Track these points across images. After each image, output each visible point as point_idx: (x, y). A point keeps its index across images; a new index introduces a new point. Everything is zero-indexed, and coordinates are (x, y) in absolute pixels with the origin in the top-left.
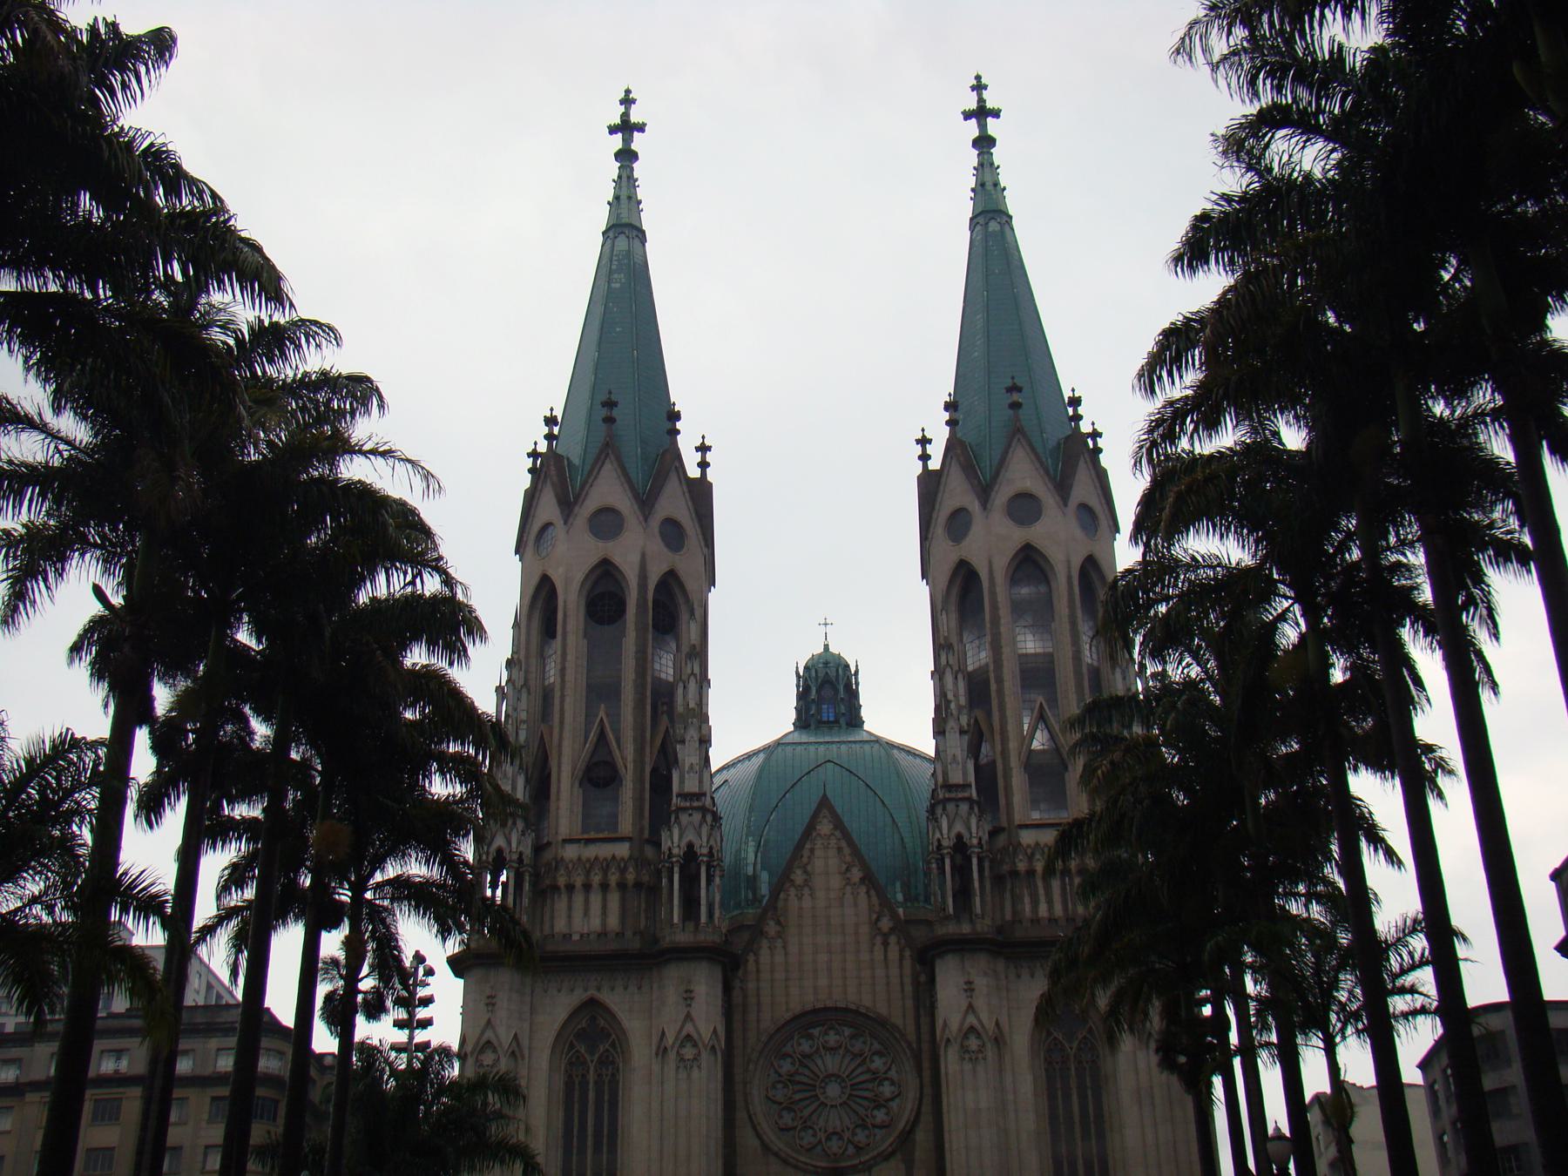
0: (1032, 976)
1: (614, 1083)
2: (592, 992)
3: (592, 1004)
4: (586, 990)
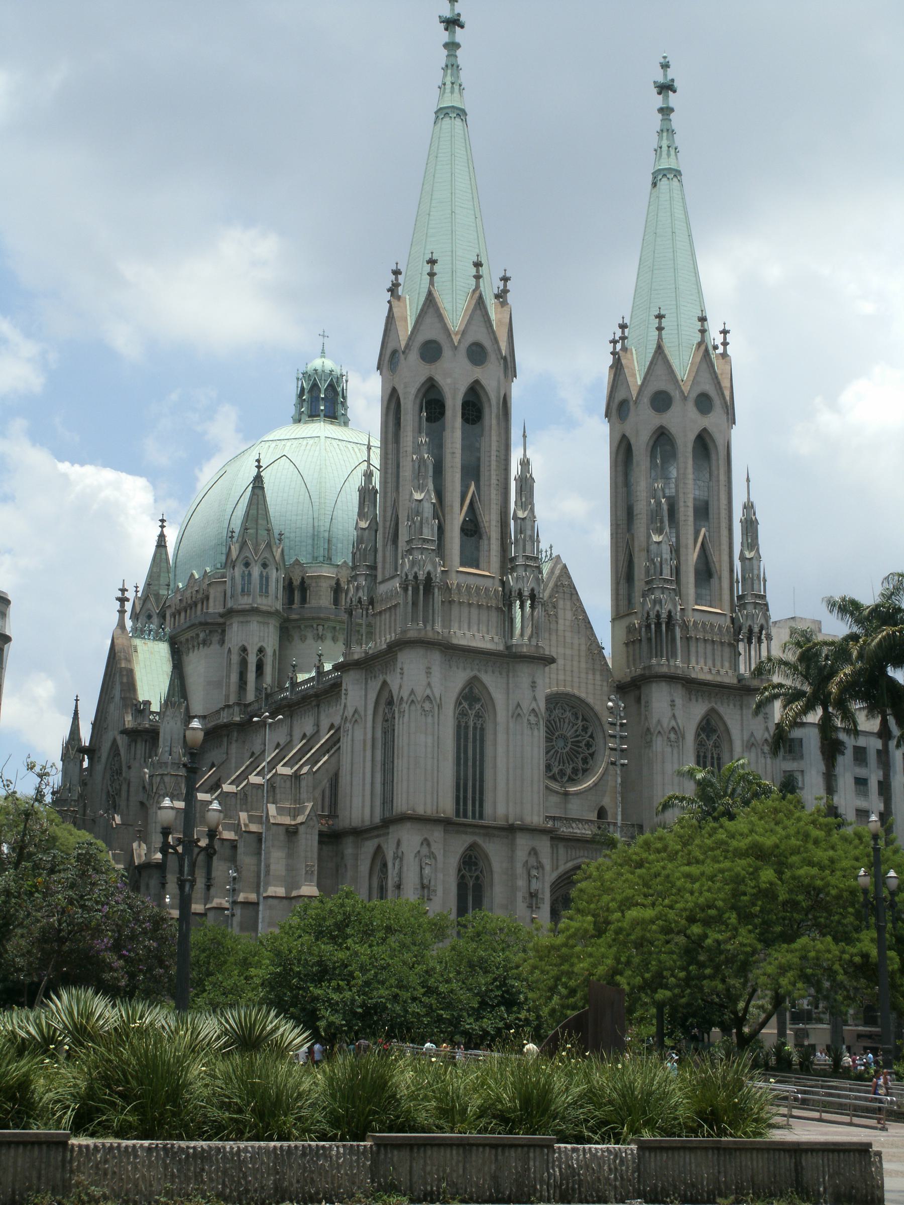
0: (697, 701)
1: (482, 729)
2: (475, 672)
3: (475, 678)
4: (472, 670)
